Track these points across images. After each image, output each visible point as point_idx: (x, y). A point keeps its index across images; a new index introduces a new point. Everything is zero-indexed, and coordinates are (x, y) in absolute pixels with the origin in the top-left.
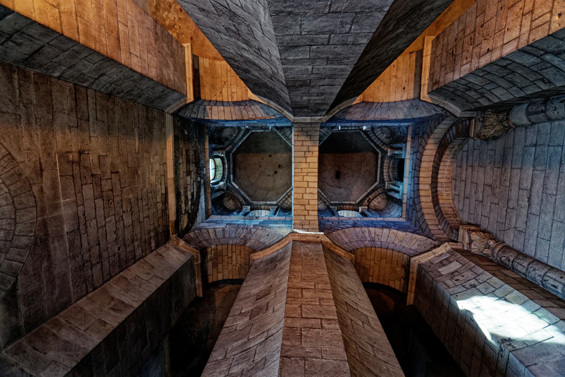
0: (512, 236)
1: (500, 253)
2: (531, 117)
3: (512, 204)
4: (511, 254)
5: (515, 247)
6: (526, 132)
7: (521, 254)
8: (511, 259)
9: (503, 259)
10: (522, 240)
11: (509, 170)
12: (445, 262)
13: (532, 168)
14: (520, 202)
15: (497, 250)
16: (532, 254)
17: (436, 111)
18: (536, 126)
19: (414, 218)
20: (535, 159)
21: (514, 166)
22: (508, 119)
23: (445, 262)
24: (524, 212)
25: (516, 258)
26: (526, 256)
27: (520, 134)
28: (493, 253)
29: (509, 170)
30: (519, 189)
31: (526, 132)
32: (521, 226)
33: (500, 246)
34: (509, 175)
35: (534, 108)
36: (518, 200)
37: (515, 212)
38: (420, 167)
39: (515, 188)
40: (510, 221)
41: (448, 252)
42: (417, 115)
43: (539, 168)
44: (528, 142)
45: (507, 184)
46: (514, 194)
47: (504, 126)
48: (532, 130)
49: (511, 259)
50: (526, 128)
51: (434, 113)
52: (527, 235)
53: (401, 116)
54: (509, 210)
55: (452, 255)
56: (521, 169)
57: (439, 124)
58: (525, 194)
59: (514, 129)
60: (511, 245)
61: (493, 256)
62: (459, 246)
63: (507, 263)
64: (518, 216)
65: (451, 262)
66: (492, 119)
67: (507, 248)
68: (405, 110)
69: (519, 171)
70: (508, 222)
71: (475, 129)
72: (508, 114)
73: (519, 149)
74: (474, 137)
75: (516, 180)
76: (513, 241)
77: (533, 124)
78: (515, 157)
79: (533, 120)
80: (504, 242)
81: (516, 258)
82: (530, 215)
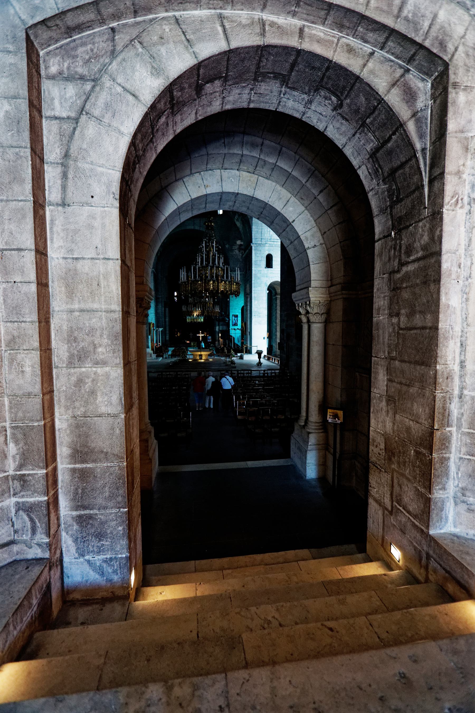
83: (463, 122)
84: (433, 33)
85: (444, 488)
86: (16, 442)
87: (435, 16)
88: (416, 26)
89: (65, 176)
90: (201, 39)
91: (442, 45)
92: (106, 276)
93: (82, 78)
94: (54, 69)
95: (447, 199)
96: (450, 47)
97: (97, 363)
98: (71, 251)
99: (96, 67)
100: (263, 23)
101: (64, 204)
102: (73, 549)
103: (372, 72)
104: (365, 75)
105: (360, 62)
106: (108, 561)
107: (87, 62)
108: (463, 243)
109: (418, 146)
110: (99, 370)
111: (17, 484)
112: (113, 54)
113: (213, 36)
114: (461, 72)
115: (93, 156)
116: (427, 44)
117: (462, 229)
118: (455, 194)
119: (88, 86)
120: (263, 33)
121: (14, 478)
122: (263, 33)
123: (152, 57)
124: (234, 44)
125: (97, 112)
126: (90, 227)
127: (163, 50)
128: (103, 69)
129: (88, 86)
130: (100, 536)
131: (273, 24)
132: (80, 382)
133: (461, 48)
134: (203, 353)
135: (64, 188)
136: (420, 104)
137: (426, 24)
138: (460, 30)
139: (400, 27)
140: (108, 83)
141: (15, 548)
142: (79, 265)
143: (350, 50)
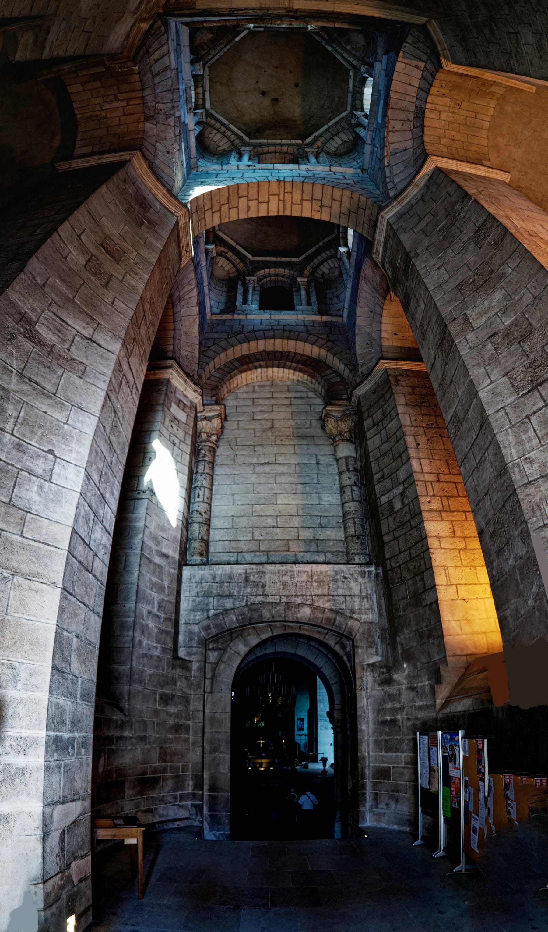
0: (227, 453)
1: (208, 448)
2: (344, 460)
3: (258, 448)
4: (210, 457)
5: (217, 458)
6: (329, 455)
7: (212, 464)
8: (206, 459)
9: (203, 452)
10: (225, 462)
11: (292, 443)
12: (181, 405)
13: (296, 462)
14: (262, 456)
15: (209, 444)
16: (216, 472)
17: (363, 365)
18: (335, 463)
19: (216, 336)
20: (305, 464)
21: (296, 447)
22: (343, 440)
23: (181, 405)
24: (255, 461)
25: (209, 462)
26: (213, 468)
27: (328, 450)
28: (205, 441)
29: (292, 443)
30: (275, 454)
31: (329, 455)
32: (240, 460)
33: (213, 446)
34: (287, 443)
35: (351, 461)
36: (264, 454)
37: (252, 453)
38: (288, 338)
39: (275, 450)
40: (241, 450)
41: (191, 402)
42: (360, 341)
43: (297, 468)
44: (320, 458)
45: (278, 443)
46: (269, 450)
47: (336, 436)
48: (331, 459)
49: (206, 459)
50: (333, 455)
51: (360, 362)
52: (233, 466)
53: (359, 321)
54: (252, 447)
55: (191, 408)
56: (295, 453)
57: (346, 365)
58: (272, 460)
59: (332, 444)
60: (217, 454)
61: (201, 442)
62: (200, 408)
63: (201, 456)
64: (249, 456)
65: (183, 410)
66: (344, 427)
67: (213, 451)
68: (368, 330)
69: (293, 452)
70: (240, 447)
71: (335, 411)
72: (347, 440)
73: (314, 449)
74: (326, 411)
75: (283, 450)
76: (222, 455)
77: (337, 460)
78: (305, 447)
79: (340, 461)
80: (217, 447)
81: (209, 462)
82: (252, 466)
83: (361, 659)
84: (347, 630)
85: (364, 806)
86: (193, 780)
87: (347, 624)
88: (340, 628)
89: (212, 683)
90: (263, 633)
91: (351, 633)
92: (226, 719)
93: (220, 649)
94: (211, 647)
95: (357, 688)
96: (354, 634)
97: (220, 753)
98: (213, 710)
99: (225, 645)
100: (285, 626)
101: (211, 692)
102: (208, 828)
103: (328, 639)
104: (325, 640)
105: (323, 636)
106: (221, 835)
107: (222, 644)
108: (366, 704)
109: (348, 665)
110: (221, 755)
111: (192, 796)
112: (231, 640)
113: (267, 632)
114: (359, 642)
115: (223, 675)
116: (345, 633)
117: (365, 699)
118: (361, 685)
119: (222, 652)
120: (285, 629)
121: (191, 794)
122: (285, 629)
123: (245, 640)
124: (275, 634)
125: (225, 660)
126: (220, 701)
127: (249, 638)
128: (228, 646)
129: (222, 652)
130: (219, 823)
131: (289, 626)
132: (214, 760)
133: (358, 634)
134: (263, 761)
135: (212, 687)
136: (348, 650)
137: (344, 627)
138: (357, 628)
139: (334, 629)
140: (229, 650)
141: (190, 821)
142: (216, 715)
143: (319, 632)
